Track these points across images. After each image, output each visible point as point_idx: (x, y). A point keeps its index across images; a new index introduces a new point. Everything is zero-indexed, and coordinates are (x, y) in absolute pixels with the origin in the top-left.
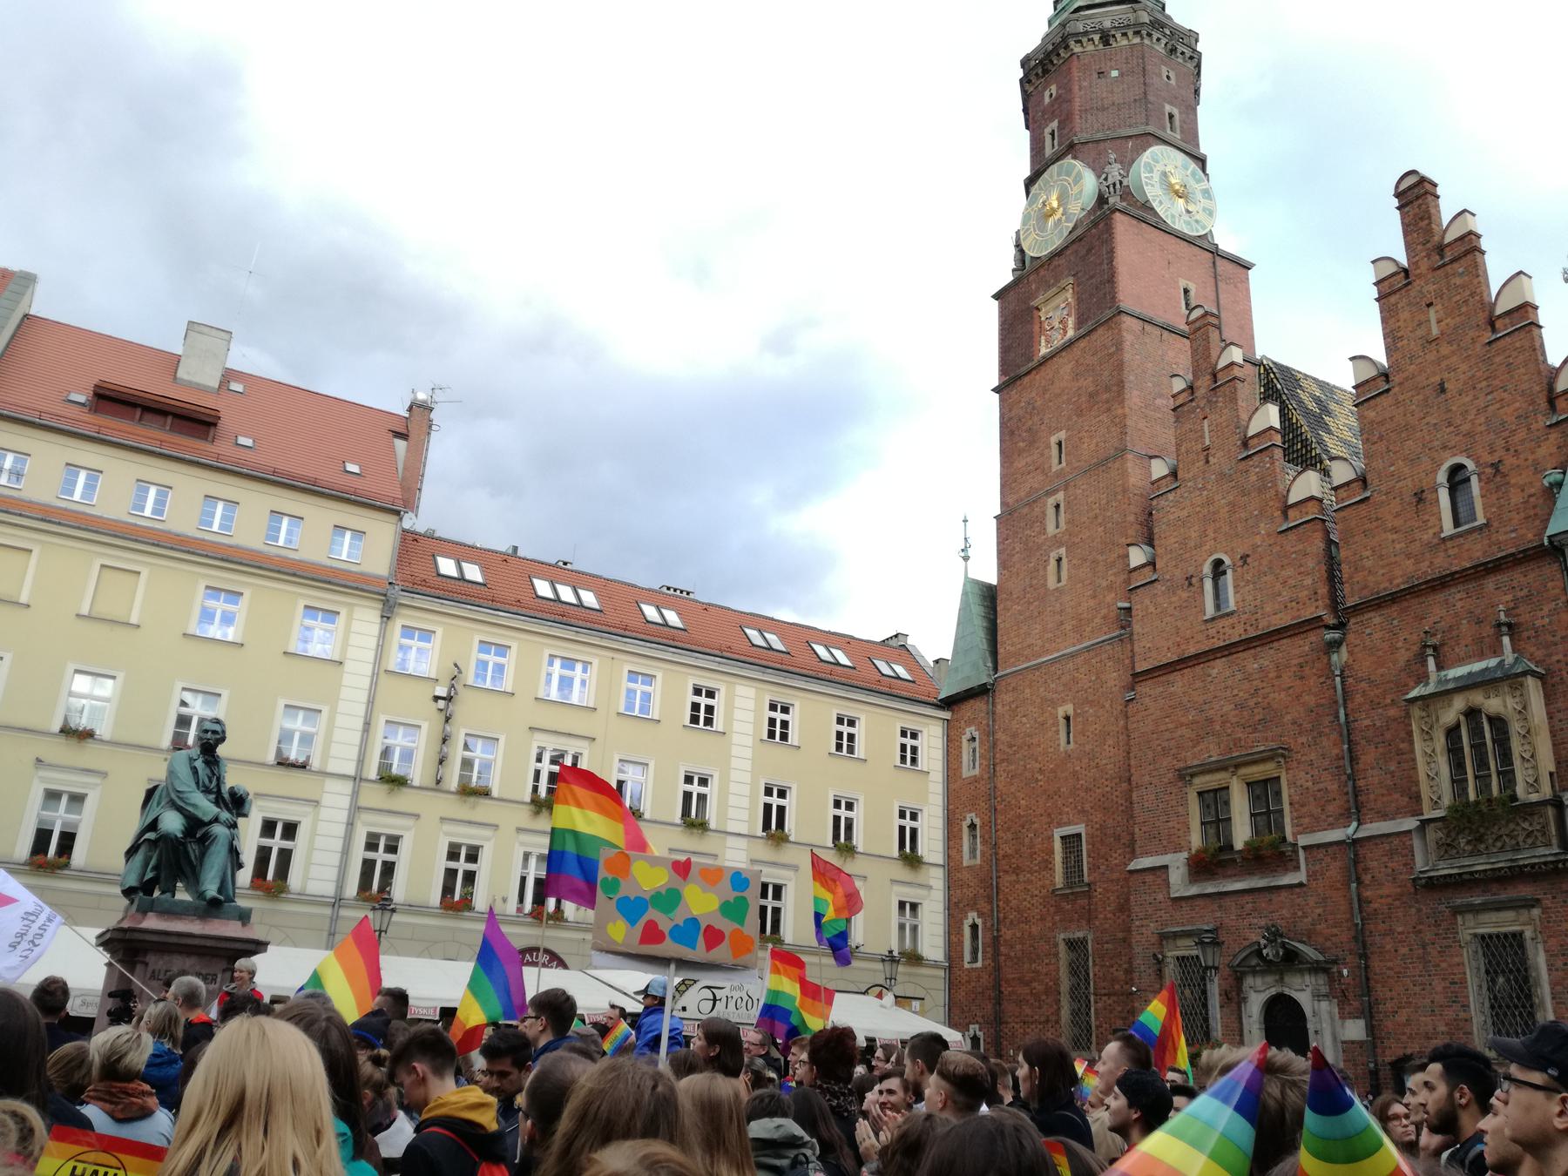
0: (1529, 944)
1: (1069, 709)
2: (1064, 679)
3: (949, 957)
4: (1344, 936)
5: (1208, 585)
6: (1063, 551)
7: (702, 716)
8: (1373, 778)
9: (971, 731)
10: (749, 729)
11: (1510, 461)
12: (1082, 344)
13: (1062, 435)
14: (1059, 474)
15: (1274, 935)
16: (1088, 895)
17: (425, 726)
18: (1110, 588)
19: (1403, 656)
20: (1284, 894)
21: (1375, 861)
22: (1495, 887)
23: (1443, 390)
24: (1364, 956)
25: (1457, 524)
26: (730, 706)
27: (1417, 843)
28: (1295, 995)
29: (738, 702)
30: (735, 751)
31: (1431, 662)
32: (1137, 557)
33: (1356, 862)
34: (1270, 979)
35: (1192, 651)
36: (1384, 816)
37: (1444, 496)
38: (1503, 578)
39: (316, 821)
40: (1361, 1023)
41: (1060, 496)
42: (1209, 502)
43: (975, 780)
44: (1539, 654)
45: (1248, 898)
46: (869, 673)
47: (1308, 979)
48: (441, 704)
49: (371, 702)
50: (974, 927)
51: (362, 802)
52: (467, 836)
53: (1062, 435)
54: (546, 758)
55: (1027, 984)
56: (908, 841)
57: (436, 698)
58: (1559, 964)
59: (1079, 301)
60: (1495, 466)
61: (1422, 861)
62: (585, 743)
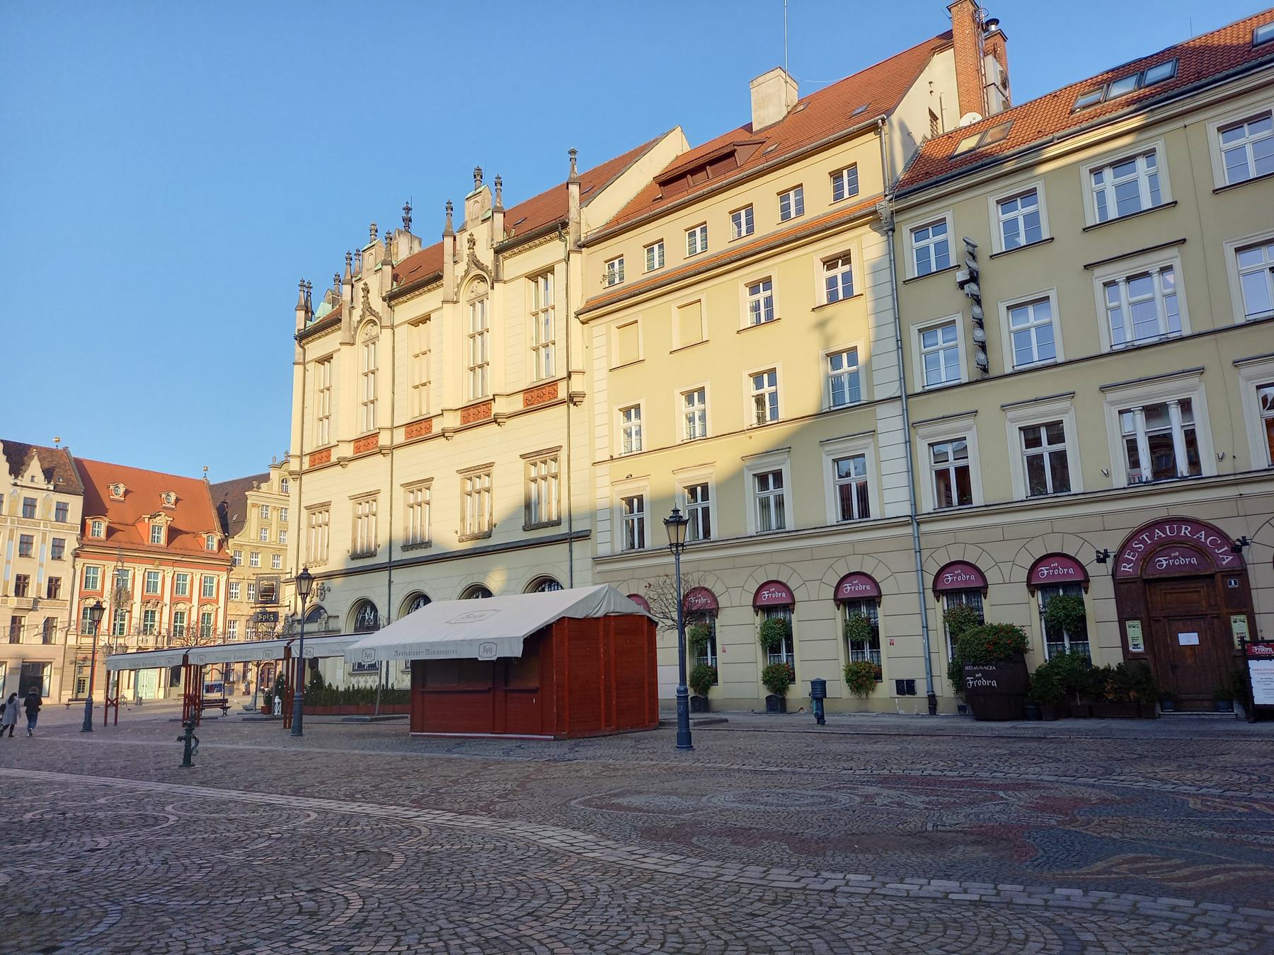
17: (959, 319)
39: (877, 448)
49: (898, 318)
51: (913, 419)
52: (1038, 415)
57: (962, 285)
62: (1173, 251)
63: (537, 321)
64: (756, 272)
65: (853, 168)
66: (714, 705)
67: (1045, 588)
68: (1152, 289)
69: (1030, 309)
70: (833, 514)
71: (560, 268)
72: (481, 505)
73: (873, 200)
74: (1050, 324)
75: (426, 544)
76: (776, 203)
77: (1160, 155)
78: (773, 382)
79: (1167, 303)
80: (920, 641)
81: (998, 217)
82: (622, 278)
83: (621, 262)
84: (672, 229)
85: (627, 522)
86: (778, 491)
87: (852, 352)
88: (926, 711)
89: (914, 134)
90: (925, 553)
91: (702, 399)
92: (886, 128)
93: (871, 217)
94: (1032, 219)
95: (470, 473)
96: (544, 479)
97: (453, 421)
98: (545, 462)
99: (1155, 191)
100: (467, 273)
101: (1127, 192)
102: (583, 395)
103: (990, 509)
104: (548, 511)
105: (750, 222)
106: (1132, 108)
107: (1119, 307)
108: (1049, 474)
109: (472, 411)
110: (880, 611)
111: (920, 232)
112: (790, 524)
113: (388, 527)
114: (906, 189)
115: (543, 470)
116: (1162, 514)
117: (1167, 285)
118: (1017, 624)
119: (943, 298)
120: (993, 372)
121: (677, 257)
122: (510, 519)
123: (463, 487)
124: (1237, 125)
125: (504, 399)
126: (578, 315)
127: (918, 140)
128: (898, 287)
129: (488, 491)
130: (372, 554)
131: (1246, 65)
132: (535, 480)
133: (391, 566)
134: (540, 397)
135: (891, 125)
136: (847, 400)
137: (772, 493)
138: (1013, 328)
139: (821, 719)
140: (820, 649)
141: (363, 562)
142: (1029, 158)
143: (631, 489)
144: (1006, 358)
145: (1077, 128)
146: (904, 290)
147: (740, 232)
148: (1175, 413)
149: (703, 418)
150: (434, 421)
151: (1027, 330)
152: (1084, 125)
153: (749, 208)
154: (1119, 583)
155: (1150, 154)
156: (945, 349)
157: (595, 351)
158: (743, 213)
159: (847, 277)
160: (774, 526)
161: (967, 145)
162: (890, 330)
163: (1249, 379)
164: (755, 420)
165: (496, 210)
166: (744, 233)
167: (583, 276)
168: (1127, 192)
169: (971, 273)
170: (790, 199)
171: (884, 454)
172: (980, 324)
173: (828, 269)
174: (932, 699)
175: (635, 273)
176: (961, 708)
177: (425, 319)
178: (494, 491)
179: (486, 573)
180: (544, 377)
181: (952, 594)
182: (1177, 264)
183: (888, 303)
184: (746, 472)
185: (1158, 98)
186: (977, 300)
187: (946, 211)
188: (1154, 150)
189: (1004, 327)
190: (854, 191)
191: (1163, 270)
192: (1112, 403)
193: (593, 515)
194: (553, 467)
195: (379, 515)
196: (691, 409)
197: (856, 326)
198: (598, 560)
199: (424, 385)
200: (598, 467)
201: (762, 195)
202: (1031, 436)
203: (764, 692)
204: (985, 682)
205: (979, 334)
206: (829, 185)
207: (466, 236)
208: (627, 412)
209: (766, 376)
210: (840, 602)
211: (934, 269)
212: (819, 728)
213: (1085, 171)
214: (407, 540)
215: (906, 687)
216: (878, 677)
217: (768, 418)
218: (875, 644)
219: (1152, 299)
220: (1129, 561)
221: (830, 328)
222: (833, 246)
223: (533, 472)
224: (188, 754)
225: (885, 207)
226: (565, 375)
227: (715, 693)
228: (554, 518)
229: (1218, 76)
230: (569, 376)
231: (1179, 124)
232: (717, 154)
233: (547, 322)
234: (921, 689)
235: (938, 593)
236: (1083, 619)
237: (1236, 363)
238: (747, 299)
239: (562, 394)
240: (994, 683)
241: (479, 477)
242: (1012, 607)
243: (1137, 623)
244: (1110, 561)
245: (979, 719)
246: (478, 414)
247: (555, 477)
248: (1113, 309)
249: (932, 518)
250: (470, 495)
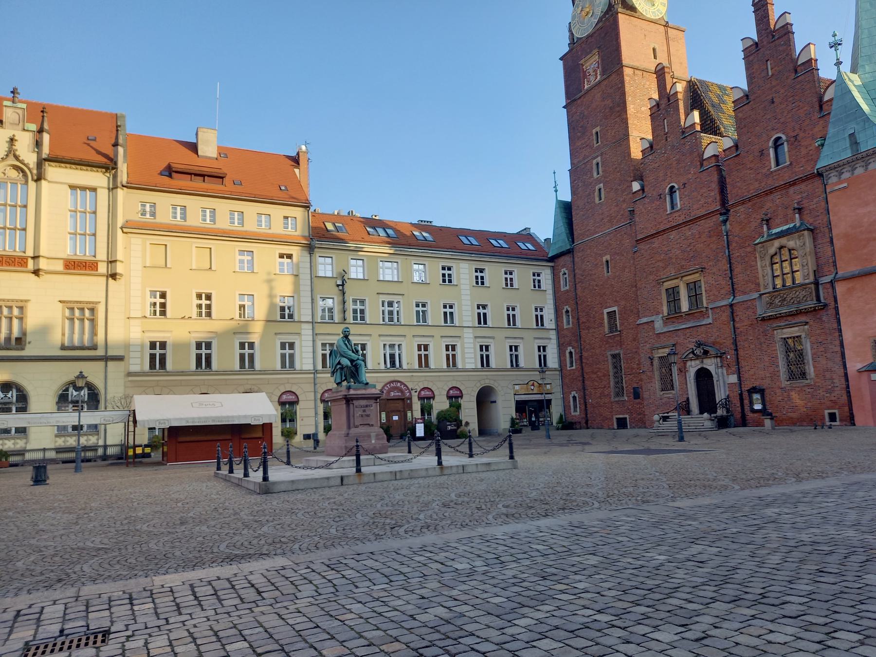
0: (803, 340)
1: (608, 257)
2: (605, 244)
3: (560, 366)
4: (729, 342)
5: (668, 198)
6: (602, 185)
7: (447, 279)
8: (739, 278)
9: (564, 270)
10: (467, 282)
11: (802, 135)
12: (605, 83)
13: (598, 129)
14: (598, 148)
15: (699, 345)
16: (620, 335)
18: (624, 201)
19: (754, 224)
20: (703, 328)
21: (740, 313)
22: (790, 318)
23: (773, 102)
24: (736, 350)
25: (778, 164)
26: (459, 274)
27: (758, 303)
28: (708, 367)
29: (462, 271)
30: (463, 292)
31: (765, 226)
32: (636, 186)
33: (732, 313)
34: (698, 362)
35: (662, 228)
36: (745, 293)
37: (772, 152)
38: (797, 188)
39: (301, 341)
40: (736, 376)
41: (599, 159)
42: (668, 159)
43: (567, 291)
44: (811, 220)
45: (688, 331)
46: (515, 248)
47: (713, 360)
48: (341, 288)
50: (571, 353)
51: (317, 332)
53: (598, 129)
54: (386, 304)
55: (595, 373)
56: (540, 320)
57: (338, 286)
58: (815, 347)
59: (602, 60)
60: (795, 137)
61: (761, 310)
110: (298, 407)
116: (392, 379)
125: (45, 260)
157: (134, 252)
193: (127, 346)
198: (130, 374)
215: (307, 437)
222: (286, 250)
235: (323, 401)
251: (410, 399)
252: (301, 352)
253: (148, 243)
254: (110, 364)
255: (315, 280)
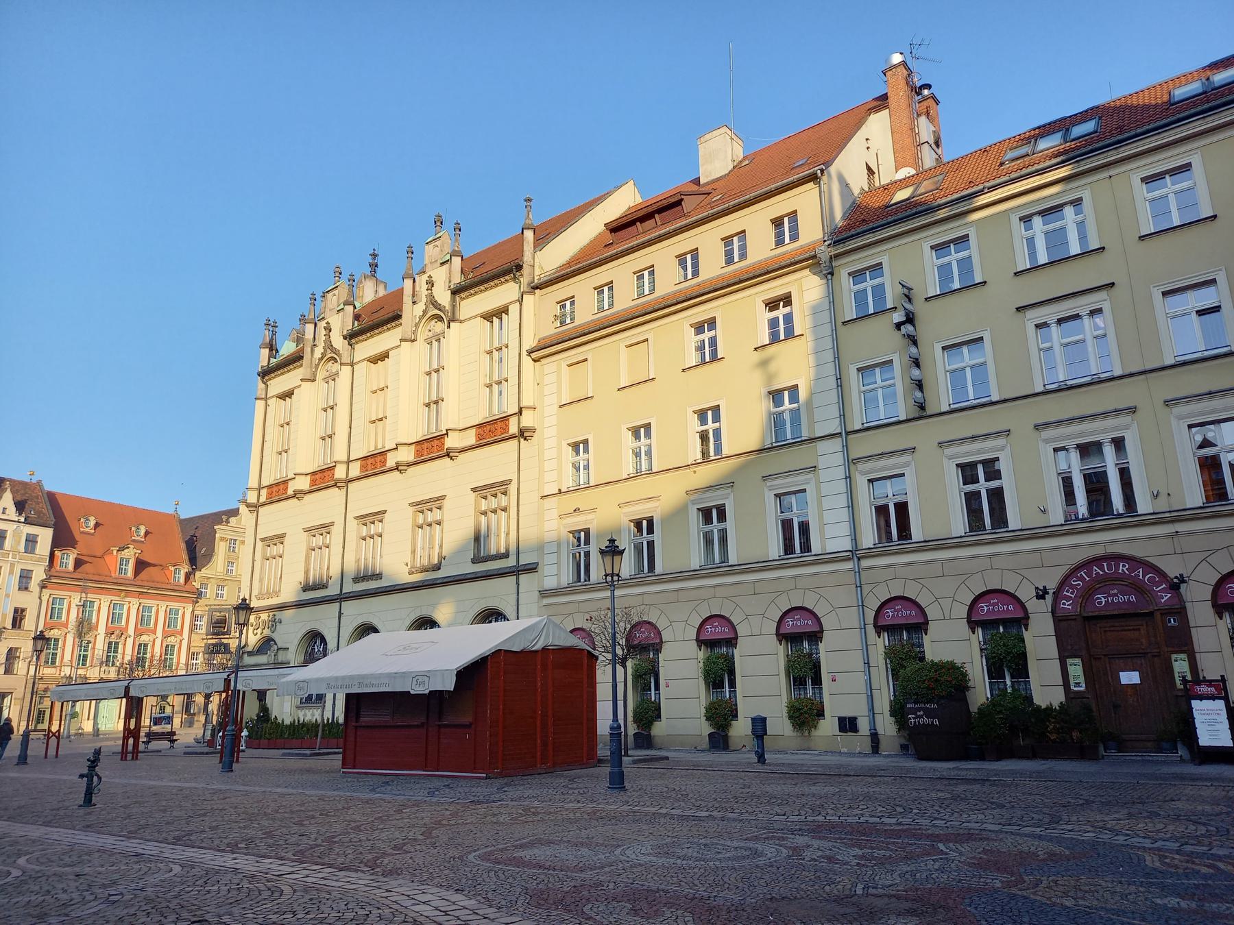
17: (896, 359)
39: (818, 483)
49: (837, 358)
57: (898, 326)
62: (1103, 295)
63: (491, 359)
64: (701, 313)
65: (793, 215)
66: (657, 741)
67: (986, 625)
68: (1082, 331)
69: (965, 349)
70: (775, 548)
71: (514, 309)
72: (432, 538)
73: (813, 245)
74: (985, 364)
75: (377, 576)
76: (721, 249)
77: (1087, 203)
78: (717, 418)
79: (1097, 345)
80: (862, 678)
81: (931, 260)
82: (572, 319)
83: (573, 303)
84: (621, 273)
85: (574, 556)
86: (722, 526)
87: (793, 390)
88: (868, 750)
89: (852, 185)
90: (866, 589)
91: (648, 435)
92: (825, 178)
93: (810, 261)
94: (965, 264)
95: (421, 506)
96: (494, 512)
97: (406, 455)
98: (495, 496)
99: (1083, 237)
100: (425, 312)
101: (1056, 238)
102: (534, 430)
103: (929, 545)
104: (497, 544)
105: (695, 265)
106: (1059, 159)
107: (1051, 348)
108: (986, 511)
109: (426, 445)
110: (822, 646)
111: (857, 275)
112: (733, 559)
113: (340, 559)
114: (844, 235)
115: (494, 503)
117: (1097, 327)
118: (958, 661)
119: (880, 338)
120: (929, 411)
121: (626, 298)
122: (460, 551)
123: (415, 520)
124: (1159, 176)
125: (457, 433)
126: (530, 353)
127: (856, 192)
128: (837, 327)
129: (439, 523)
130: (323, 586)
131: (1166, 121)
132: (485, 513)
133: (341, 598)
134: (492, 432)
135: (829, 175)
136: (789, 436)
137: (715, 526)
138: (948, 368)
139: (761, 758)
140: (762, 683)
141: (315, 594)
142: (963, 205)
143: (579, 522)
144: (942, 397)
145: (1007, 178)
146: (841, 329)
147: (686, 275)
148: (1109, 450)
149: (649, 453)
150: (389, 455)
151: (963, 369)
152: (1014, 175)
153: (695, 253)
154: (1059, 620)
155: (1077, 202)
156: (883, 388)
157: (545, 389)
158: (689, 257)
159: (789, 318)
160: (717, 560)
161: (902, 195)
162: (830, 369)
163: (1180, 418)
164: (699, 456)
165: (454, 253)
166: (690, 276)
167: (536, 316)
168: (1056, 238)
169: (907, 315)
170: (733, 244)
171: (825, 489)
172: (917, 363)
173: (771, 310)
174: (875, 737)
175: (586, 312)
176: (904, 747)
177: (384, 356)
178: (445, 524)
179: (434, 606)
180: (497, 413)
181: (892, 629)
182: (1106, 307)
183: (828, 343)
184: (690, 506)
185: (1082, 150)
186: (914, 341)
187: (882, 255)
188: (1081, 199)
189: (939, 366)
190: (794, 237)
191: (1093, 313)
192: (1047, 441)
193: (541, 547)
194: (503, 500)
195: (332, 547)
196: (638, 444)
197: (798, 365)
198: (544, 593)
199: (380, 420)
200: (546, 500)
201: (707, 241)
202: (968, 472)
203: (707, 729)
204: (927, 721)
205: (916, 373)
206: (770, 232)
207: (425, 277)
208: (575, 447)
209: (710, 413)
210: (782, 637)
211: (871, 311)
212: (760, 767)
213: (1015, 219)
214: (359, 571)
215: (848, 725)
216: (821, 714)
217: (712, 453)
218: (817, 681)
219: (1083, 341)
220: (1068, 598)
221: (773, 367)
222: (775, 288)
223: (484, 505)
224: (89, 793)
225: (824, 252)
226: (516, 410)
227: (658, 729)
228: (503, 550)
229: (1139, 131)
230: (520, 413)
231: (1106, 174)
232: (665, 203)
233: (501, 360)
234: (864, 726)
235: (879, 629)
236: (1023, 656)
237: (1167, 403)
238: (692, 339)
239: (513, 429)
240: (936, 722)
241: (431, 510)
242: (953, 643)
243: (1078, 661)
244: (1049, 598)
245: (921, 759)
246: (431, 448)
247: (504, 510)
248: (1045, 350)
249: (872, 553)
250: (421, 527)
251: (1180, 611)
252: (821, 511)
253: (564, 365)
254: (523, 578)
255: (841, 329)
